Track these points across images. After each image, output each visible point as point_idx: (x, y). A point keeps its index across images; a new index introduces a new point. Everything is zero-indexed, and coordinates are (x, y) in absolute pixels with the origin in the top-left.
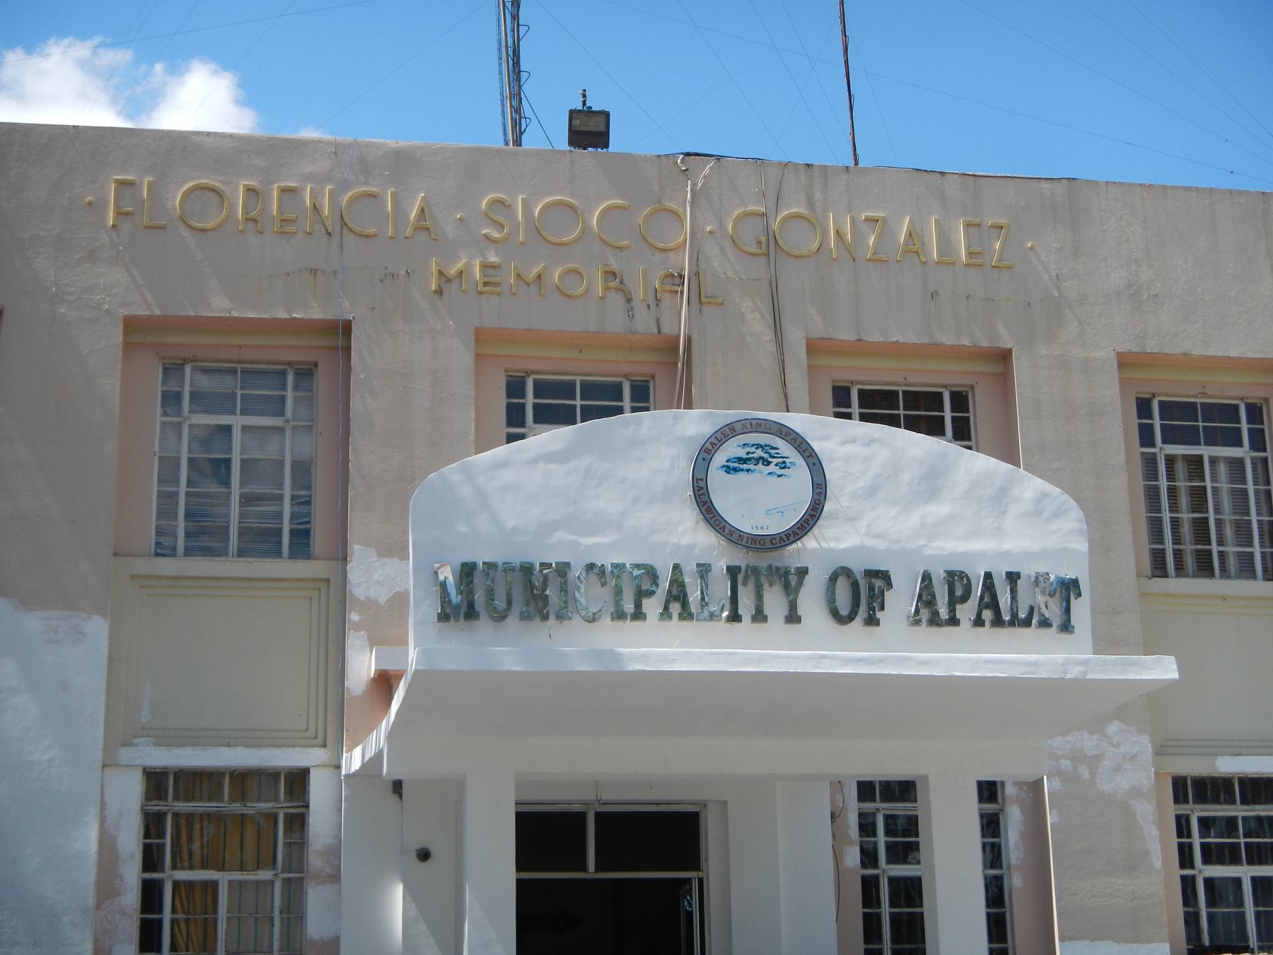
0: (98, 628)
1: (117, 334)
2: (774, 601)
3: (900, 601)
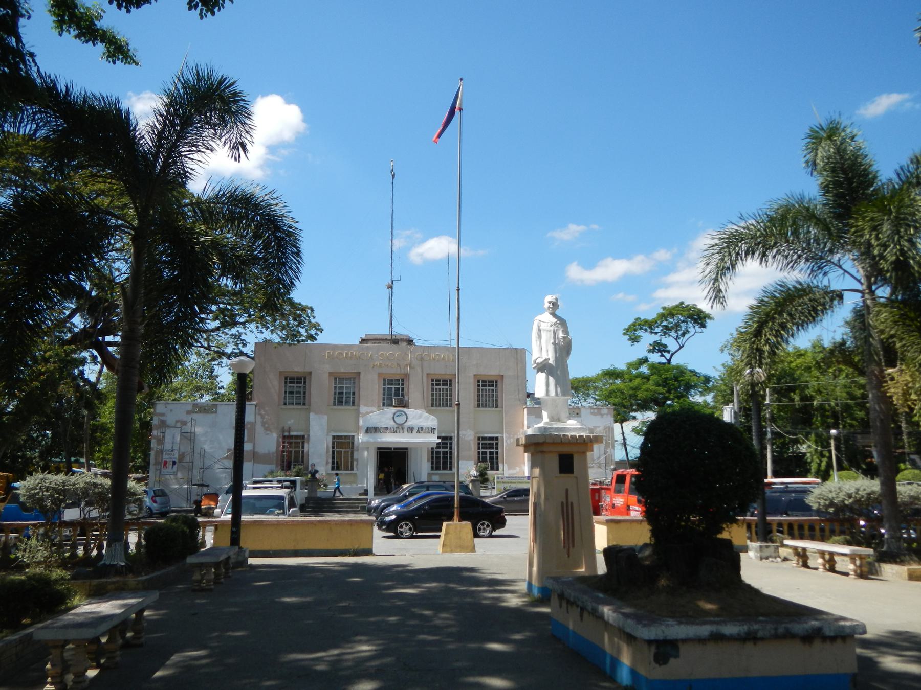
0: (326, 417)
3: (415, 431)
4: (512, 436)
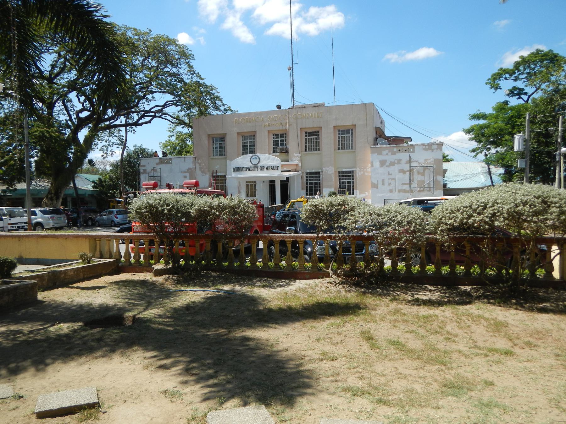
1: (236, 134)
2: (256, 169)
4: (362, 169)
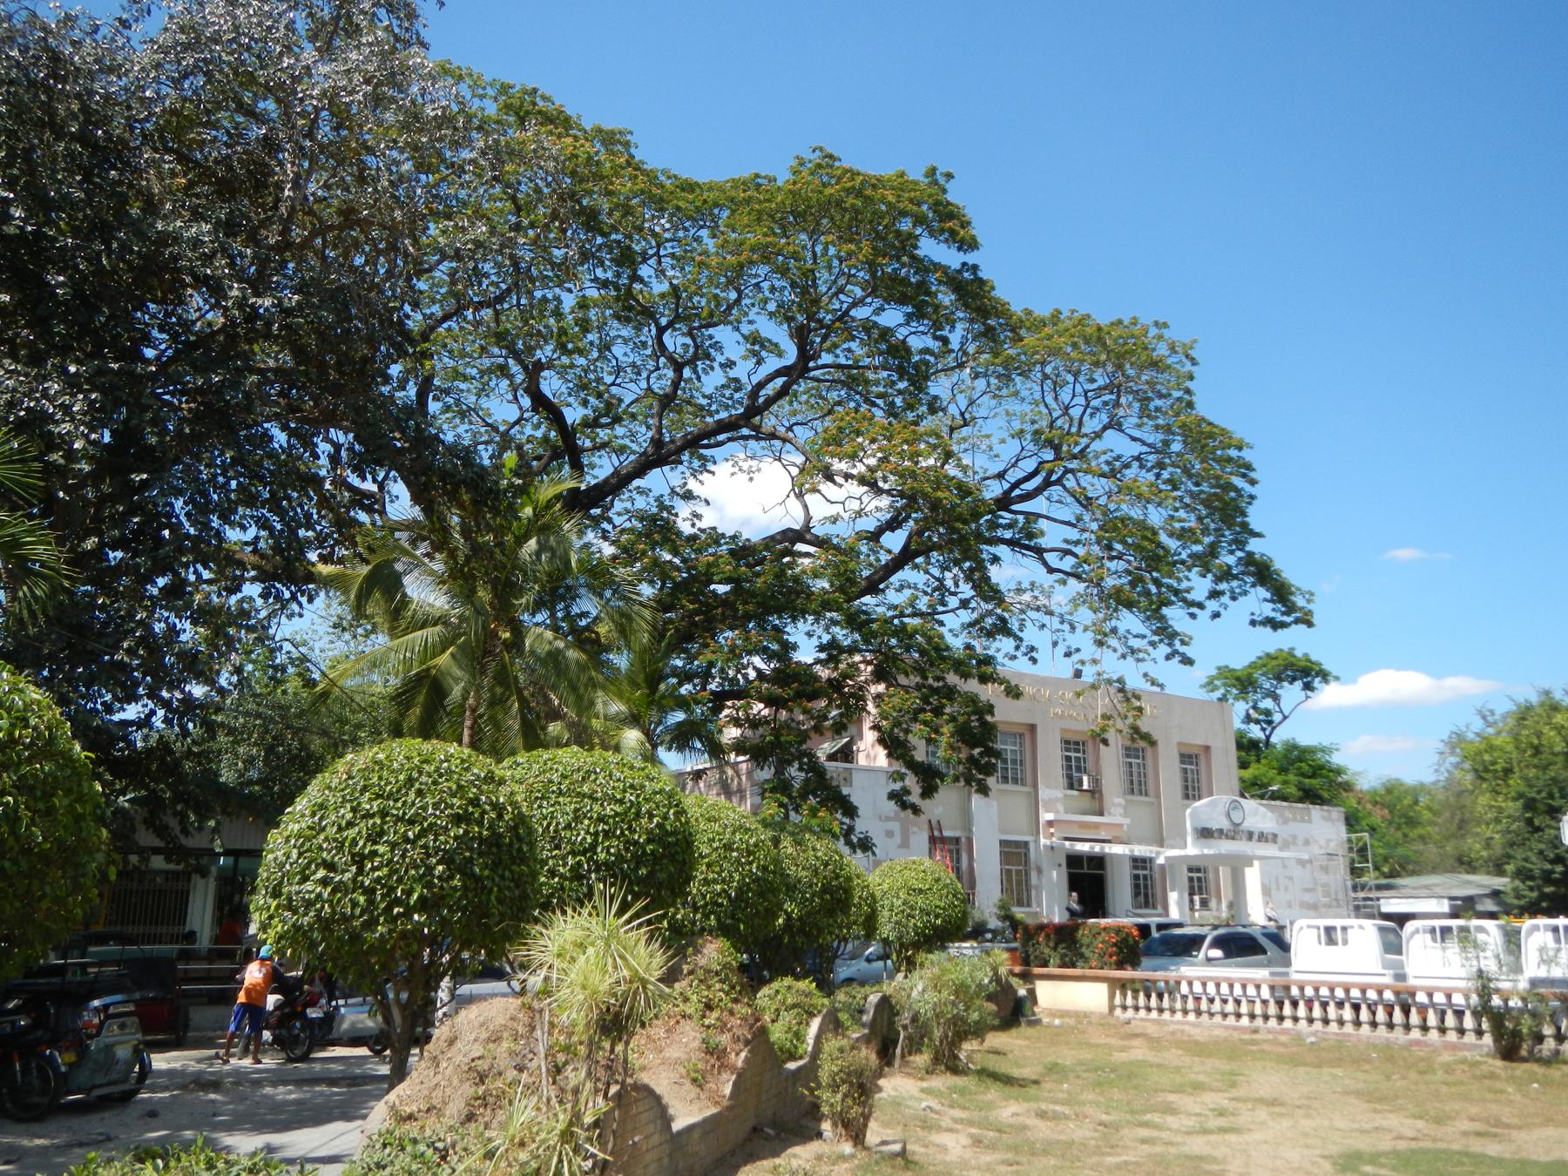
3: (1256, 837)
